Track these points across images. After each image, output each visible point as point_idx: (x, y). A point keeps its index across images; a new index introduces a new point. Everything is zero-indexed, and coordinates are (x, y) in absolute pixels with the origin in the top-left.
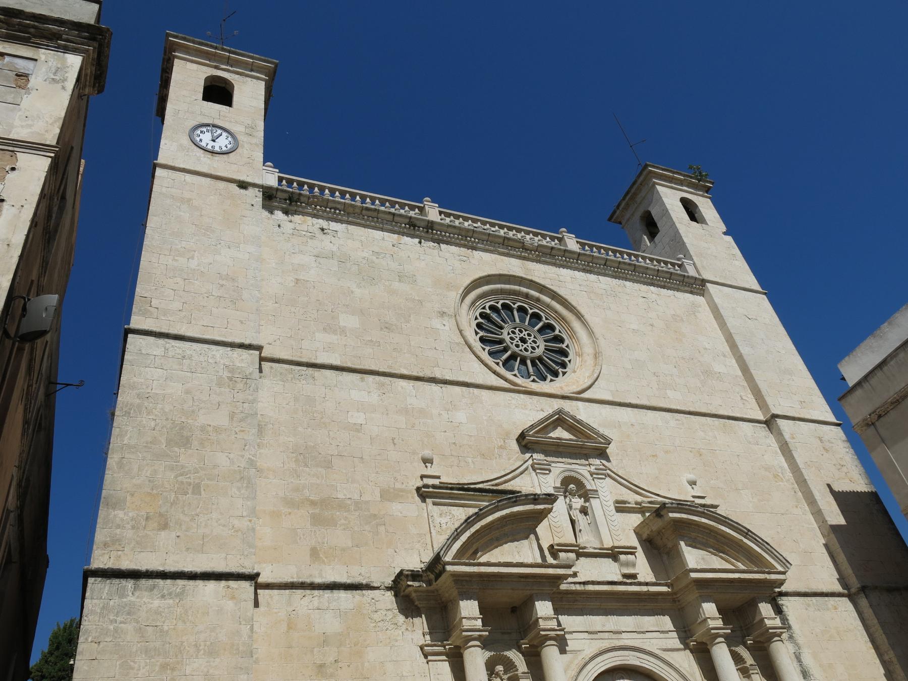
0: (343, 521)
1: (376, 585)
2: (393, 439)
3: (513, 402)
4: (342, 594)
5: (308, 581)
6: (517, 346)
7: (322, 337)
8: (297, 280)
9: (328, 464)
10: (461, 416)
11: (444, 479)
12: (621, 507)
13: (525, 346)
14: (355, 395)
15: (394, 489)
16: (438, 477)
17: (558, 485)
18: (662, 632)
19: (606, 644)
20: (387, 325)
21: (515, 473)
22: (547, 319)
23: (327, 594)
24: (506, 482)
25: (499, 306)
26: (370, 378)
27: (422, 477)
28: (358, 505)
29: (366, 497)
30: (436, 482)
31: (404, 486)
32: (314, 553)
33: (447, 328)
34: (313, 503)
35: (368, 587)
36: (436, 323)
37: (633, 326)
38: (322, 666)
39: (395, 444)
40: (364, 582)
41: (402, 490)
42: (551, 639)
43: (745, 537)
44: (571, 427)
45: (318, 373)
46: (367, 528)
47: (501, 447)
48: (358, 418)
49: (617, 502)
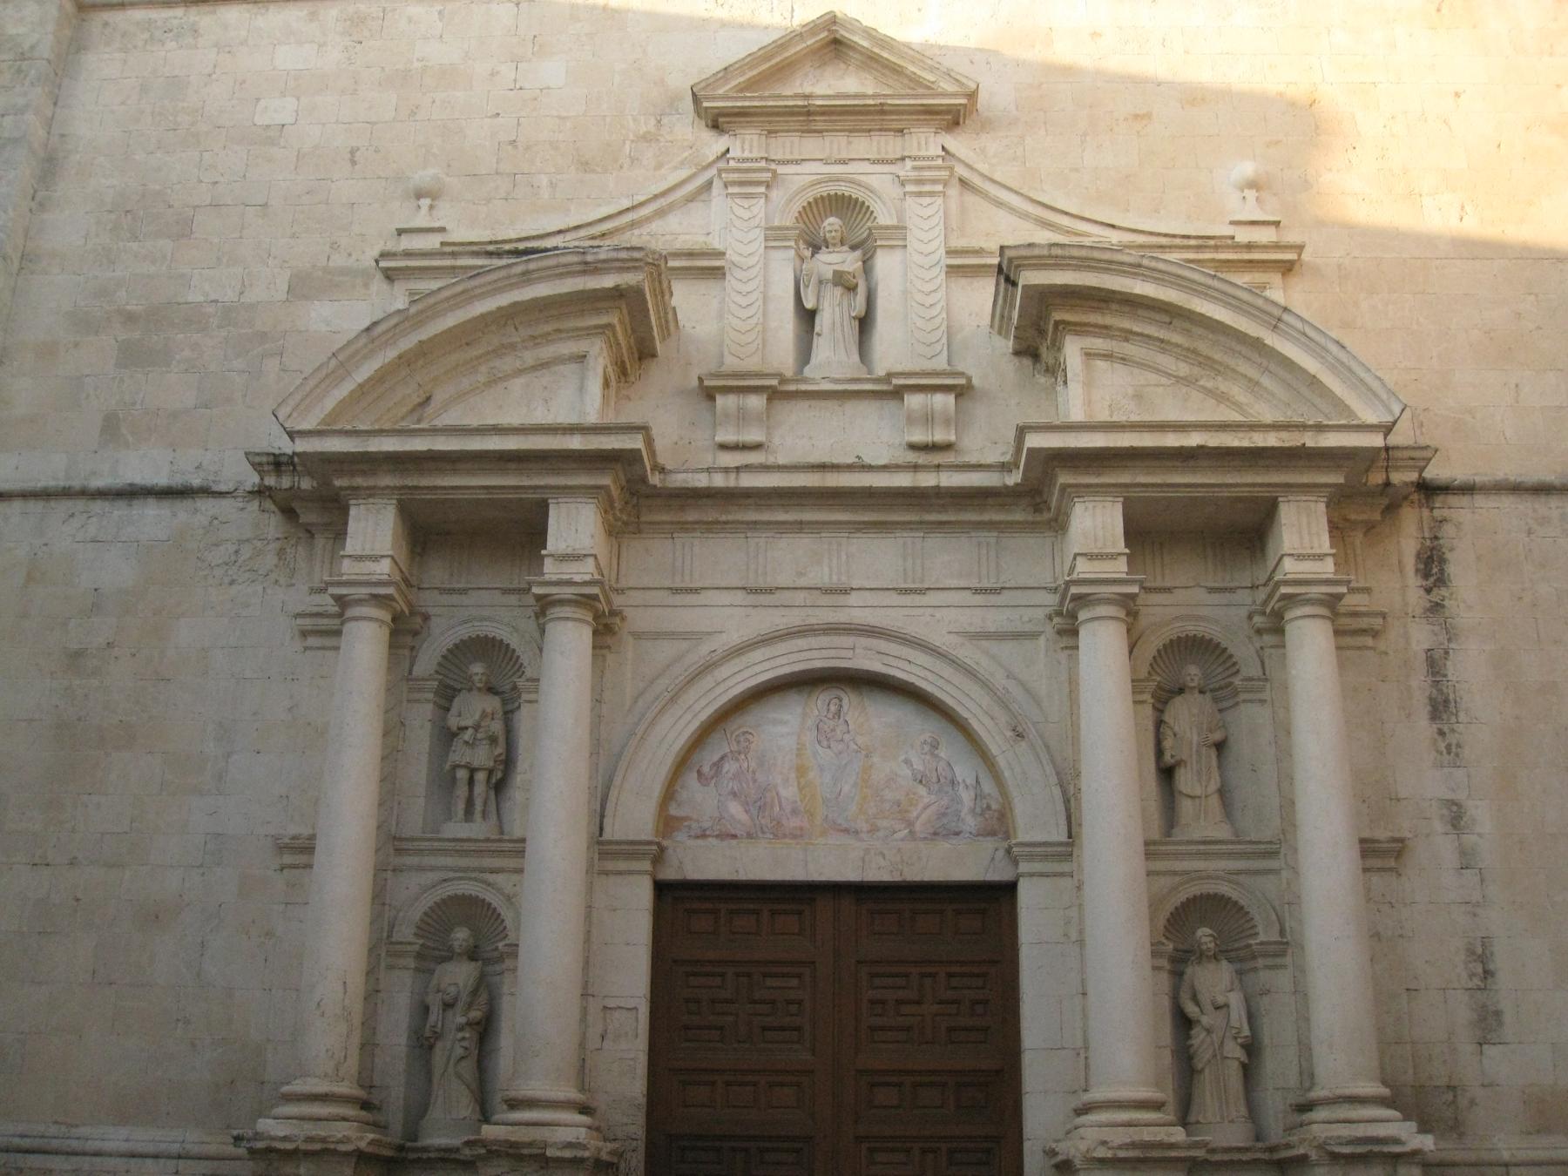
0: (187, 353)
1: (223, 488)
4: (151, 510)
5: (76, 484)
9: (184, 229)
11: (460, 234)
12: (961, 269)
16: (442, 230)
17: (789, 221)
18: (977, 591)
19: (794, 618)
21: (664, 203)
23: (119, 510)
24: (633, 225)
27: (400, 232)
29: (249, 298)
30: (432, 242)
32: (111, 427)
34: (130, 318)
35: (205, 492)
38: (78, 654)
39: (354, 163)
40: (196, 482)
41: (344, 271)
42: (562, 602)
44: (871, 58)
47: (646, 138)
48: (276, 110)
49: (951, 253)
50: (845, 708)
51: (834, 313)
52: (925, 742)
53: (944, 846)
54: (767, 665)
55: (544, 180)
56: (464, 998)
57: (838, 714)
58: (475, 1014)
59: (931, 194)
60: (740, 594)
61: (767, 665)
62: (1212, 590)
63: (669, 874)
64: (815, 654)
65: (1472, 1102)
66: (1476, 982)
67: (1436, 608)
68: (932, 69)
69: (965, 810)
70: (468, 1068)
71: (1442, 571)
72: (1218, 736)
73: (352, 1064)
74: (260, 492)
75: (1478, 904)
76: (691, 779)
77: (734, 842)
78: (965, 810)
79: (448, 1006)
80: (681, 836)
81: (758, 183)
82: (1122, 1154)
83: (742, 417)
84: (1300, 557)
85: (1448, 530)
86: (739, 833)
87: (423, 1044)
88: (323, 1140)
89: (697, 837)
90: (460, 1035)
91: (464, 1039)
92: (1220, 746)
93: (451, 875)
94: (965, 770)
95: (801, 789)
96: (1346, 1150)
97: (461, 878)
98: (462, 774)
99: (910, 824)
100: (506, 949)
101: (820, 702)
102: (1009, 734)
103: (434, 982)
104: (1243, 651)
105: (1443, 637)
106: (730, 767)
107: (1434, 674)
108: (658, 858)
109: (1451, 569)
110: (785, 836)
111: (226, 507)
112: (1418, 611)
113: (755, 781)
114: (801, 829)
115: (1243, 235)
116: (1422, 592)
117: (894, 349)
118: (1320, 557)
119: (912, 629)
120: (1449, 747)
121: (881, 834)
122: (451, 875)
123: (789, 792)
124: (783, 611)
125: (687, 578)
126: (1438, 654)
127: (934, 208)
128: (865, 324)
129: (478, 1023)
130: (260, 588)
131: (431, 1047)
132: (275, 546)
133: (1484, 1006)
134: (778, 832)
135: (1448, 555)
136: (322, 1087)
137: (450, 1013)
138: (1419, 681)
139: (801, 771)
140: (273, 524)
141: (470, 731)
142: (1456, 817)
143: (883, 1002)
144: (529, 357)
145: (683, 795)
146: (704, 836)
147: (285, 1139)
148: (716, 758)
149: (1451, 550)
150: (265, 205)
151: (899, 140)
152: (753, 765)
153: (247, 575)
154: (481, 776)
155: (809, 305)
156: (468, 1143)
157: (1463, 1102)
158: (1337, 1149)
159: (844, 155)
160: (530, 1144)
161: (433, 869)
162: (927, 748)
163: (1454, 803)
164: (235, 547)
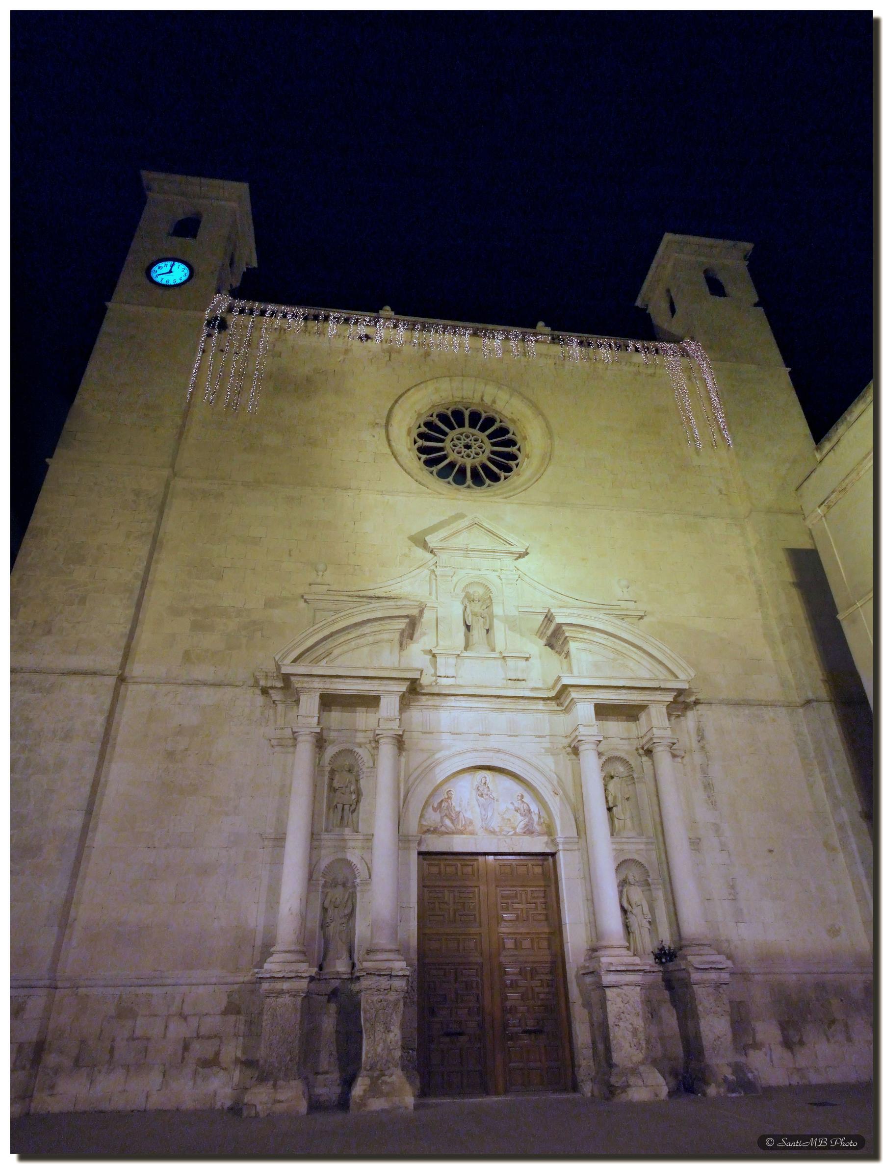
13: (468, 451)
25: (449, 413)
32: (187, 657)
34: (195, 611)
39: (290, 555)
47: (405, 555)
58: (346, 912)
63: (424, 849)
66: (731, 897)
67: (703, 748)
76: (430, 809)
84: (659, 728)
88: (297, 971)
94: (534, 808)
98: (340, 806)
102: (552, 794)
115: (623, 604)
118: (666, 729)
142: (717, 829)
144: (371, 639)
145: (427, 816)
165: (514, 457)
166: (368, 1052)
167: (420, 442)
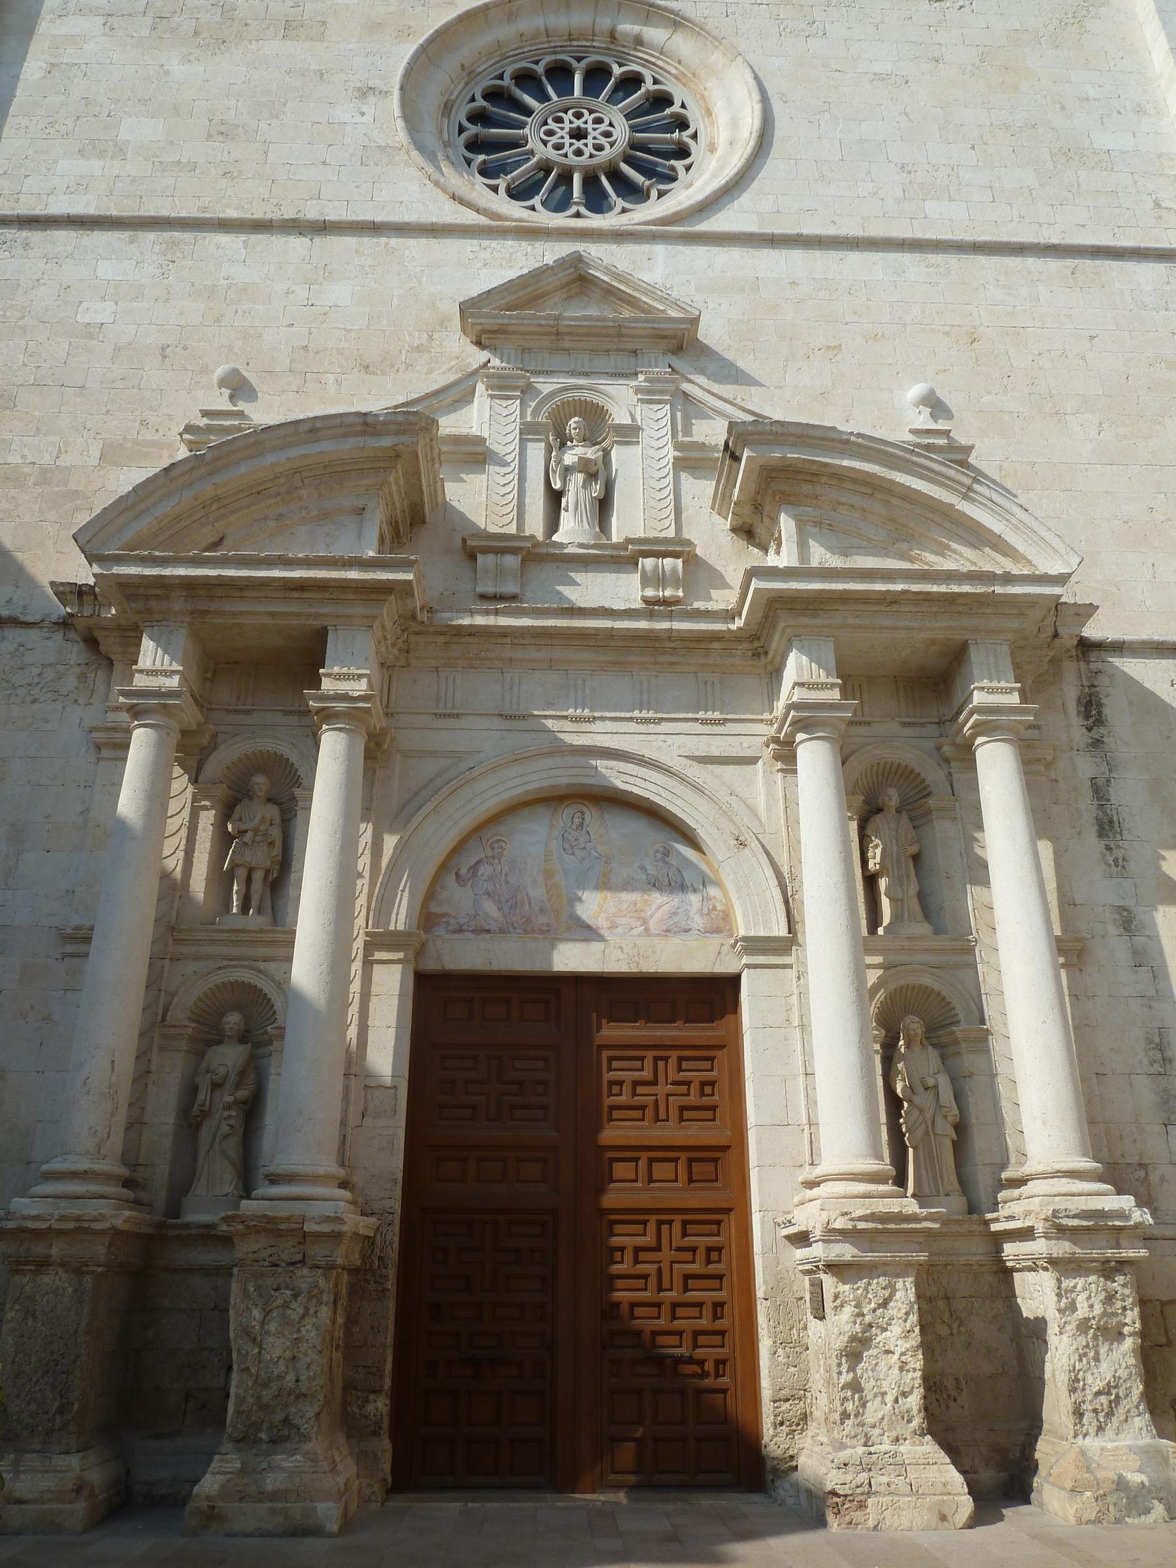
1: (30, 619)
2: (163, 349)
3: (485, 255)
6: (579, 153)
7: (71, 167)
8: (53, 65)
10: (339, 293)
14: (107, 270)
15: (135, 442)
20: (223, 128)
22: (656, 82)
26: (150, 237)
28: (45, 475)
31: (157, 437)
33: (368, 118)
36: (345, 112)
37: (884, 67)
39: (165, 357)
41: (151, 444)
43: (965, 497)
45: (36, 236)
46: (51, 515)
48: (98, 312)
50: (587, 820)
51: (576, 492)
52: (657, 851)
53: (676, 941)
54: (518, 781)
55: (331, 378)
56: (233, 1078)
57: (582, 825)
58: (242, 1094)
59: (660, 402)
60: (496, 718)
61: (518, 781)
62: (904, 724)
63: (430, 965)
64: (562, 772)
65: (1163, 1179)
66: (1157, 1068)
67: (1097, 743)
68: (660, 300)
69: (694, 911)
70: (232, 1147)
71: (1100, 713)
72: (914, 849)
73: (117, 1142)
74: (65, 624)
75: (1151, 998)
76: (451, 881)
77: (488, 936)
78: (694, 911)
79: (216, 1086)
80: (440, 931)
81: (515, 388)
82: (862, 1225)
83: (499, 573)
85: (1103, 681)
86: (492, 928)
87: (191, 1120)
88: (78, 1219)
89: (455, 932)
90: (226, 1114)
91: (230, 1117)
92: (916, 858)
93: (225, 963)
95: (548, 891)
96: (1075, 1222)
97: (234, 966)
99: (645, 922)
100: (275, 1032)
101: (566, 815)
103: (204, 1065)
104: (934, 775)
105: (1104, 768)
106: (485, 871)
107: (1099, 799)
108: (420, 953)
109: (1107, 712)
110: (533, 931)
111: (33, 633)
112: (1082, 746)
113: (507, 882)
114: (548, 925)
116: (1084, 730)
117: (628, 523)
119: (648, 752)
120: (1116, 861)
121: (619, 930)
122: (225, 963)
123: (537, 893)
124: (534, 735)
125: (450, 705)
126: (1101, 782)
127: (663, 412)
128: (604, 506)
129: (245, 1103)
130: (60, 706)
131: (198, 1126)
132: (77, 670)
133: (1165, 1090)
134: (526, 927)
135: (1104, 701)
136: (83, 1165)
137: (218, 1094)
138: (1086, 803)
139: (548, 875)
140: (76, 652)
141: (250, 834)
143: (620, 1083)
146: (460, 931)
147: (37, 1218)
148: (473, 861)
149: (1107, 696)
150: (83, 387)
151: (633, 359)
152: (506, 868)
153: (49, 695)
154: (258, 876)
155: (557, 485)
156: (225, 1219)
157: (1154, 1178)
158: (1064, 1221)
159: (588, 370)
160: (287, 1219)
161: (208, 957)
162: (659, 856)
163: (1124, 909)
164: (39, 670)
165: (682, 152)
166: (241, 1400)
167: (473, 130)
